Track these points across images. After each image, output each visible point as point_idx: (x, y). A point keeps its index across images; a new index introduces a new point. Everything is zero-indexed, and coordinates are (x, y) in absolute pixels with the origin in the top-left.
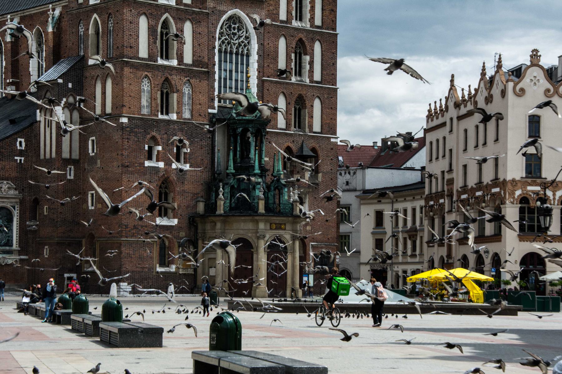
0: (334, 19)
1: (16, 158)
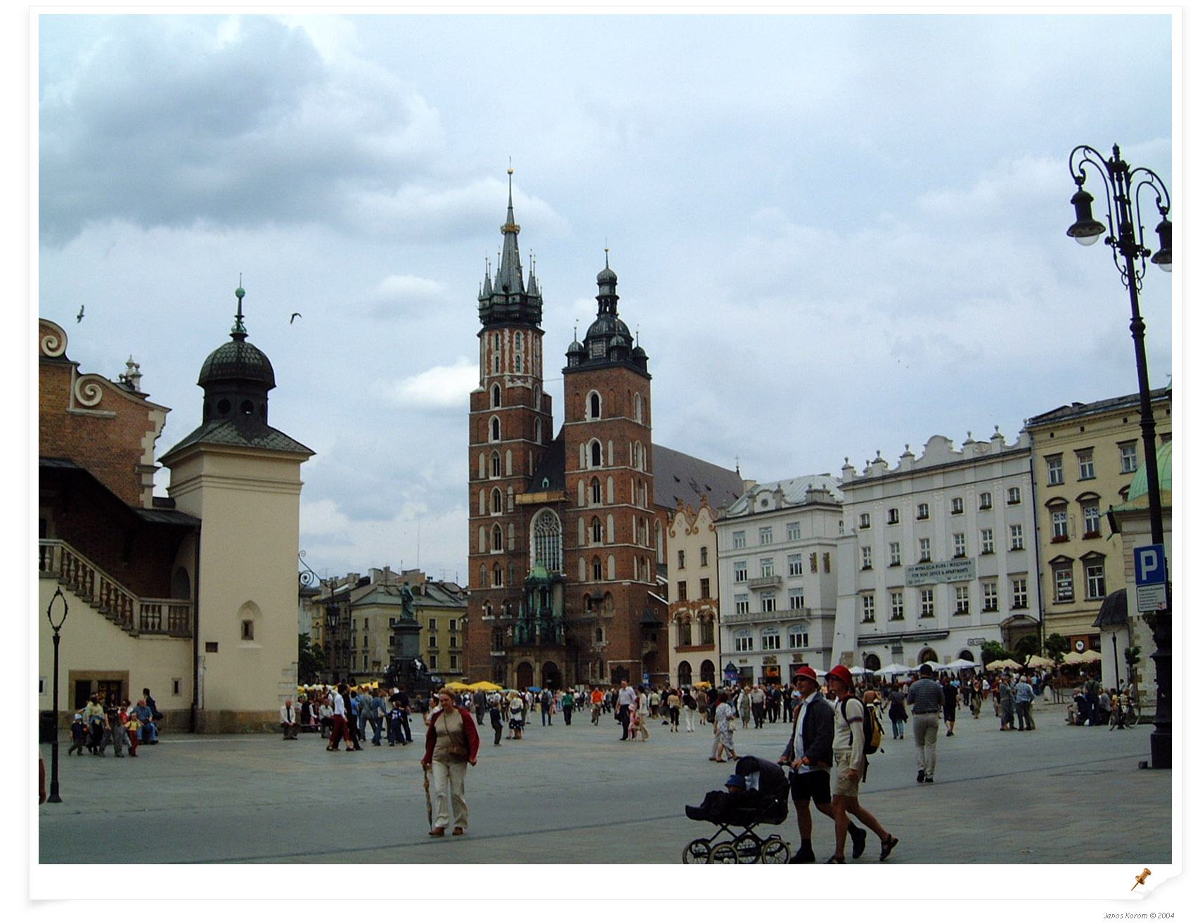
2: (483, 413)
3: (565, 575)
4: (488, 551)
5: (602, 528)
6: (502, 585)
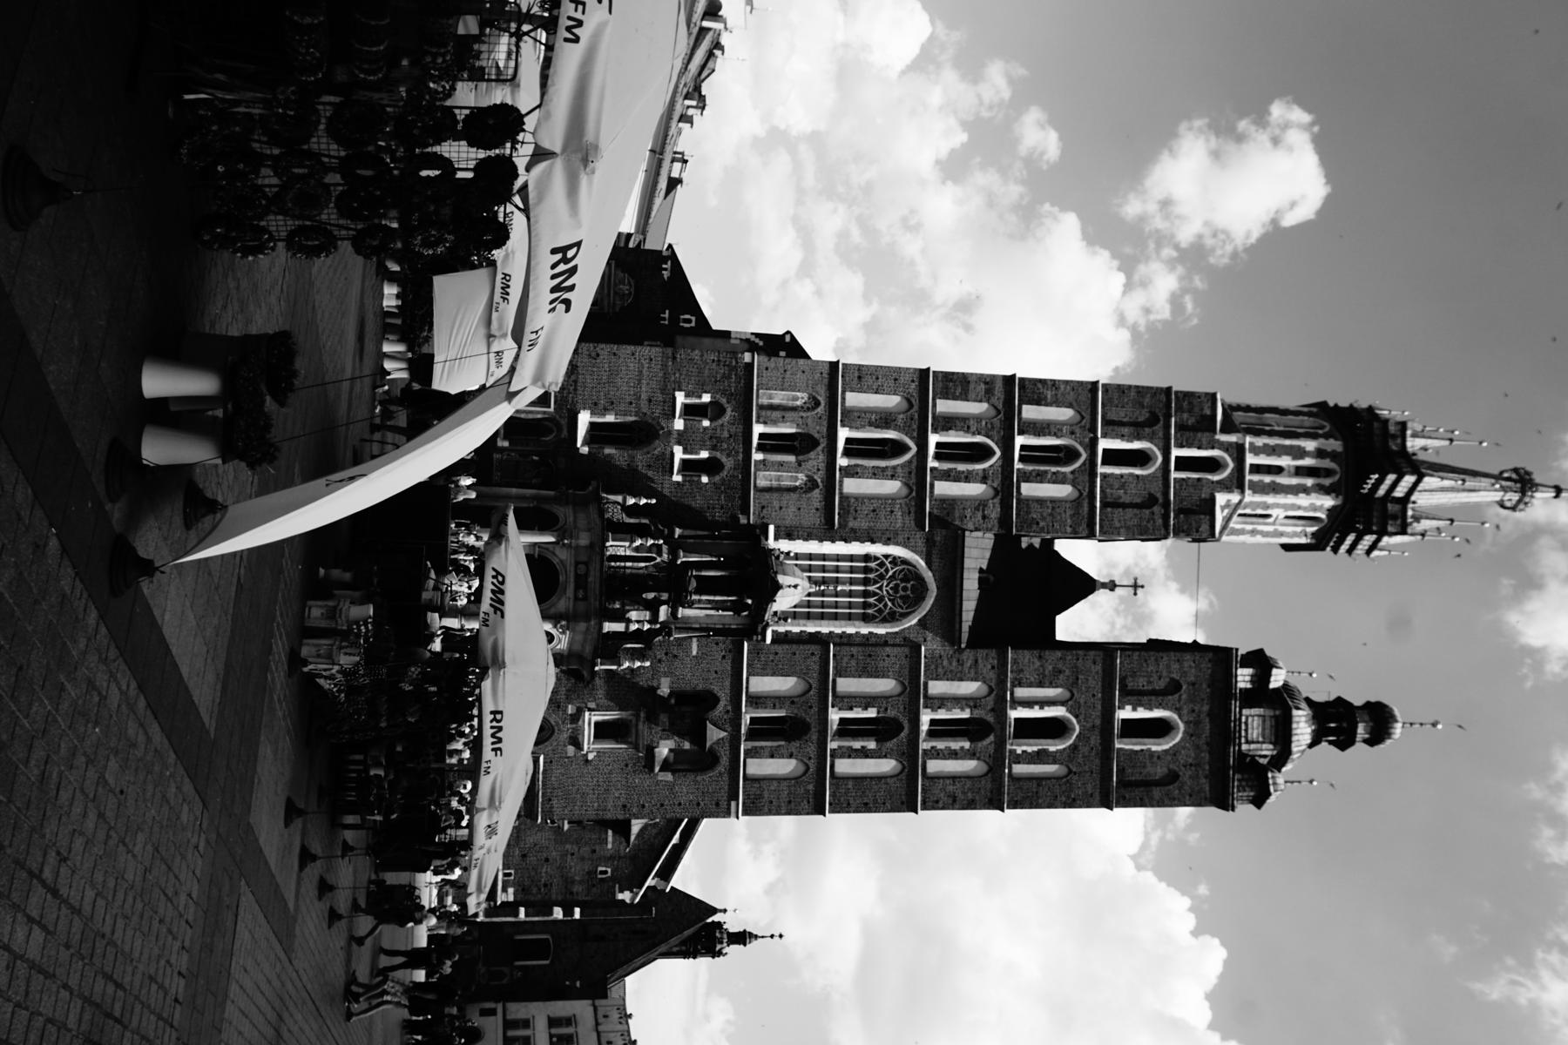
0: (941, 805)
1: (667, 312)
2: (1167, 427)
3: (769, 640)
4: (854, 417)
5: (872, 745)
6: (757, 456)
